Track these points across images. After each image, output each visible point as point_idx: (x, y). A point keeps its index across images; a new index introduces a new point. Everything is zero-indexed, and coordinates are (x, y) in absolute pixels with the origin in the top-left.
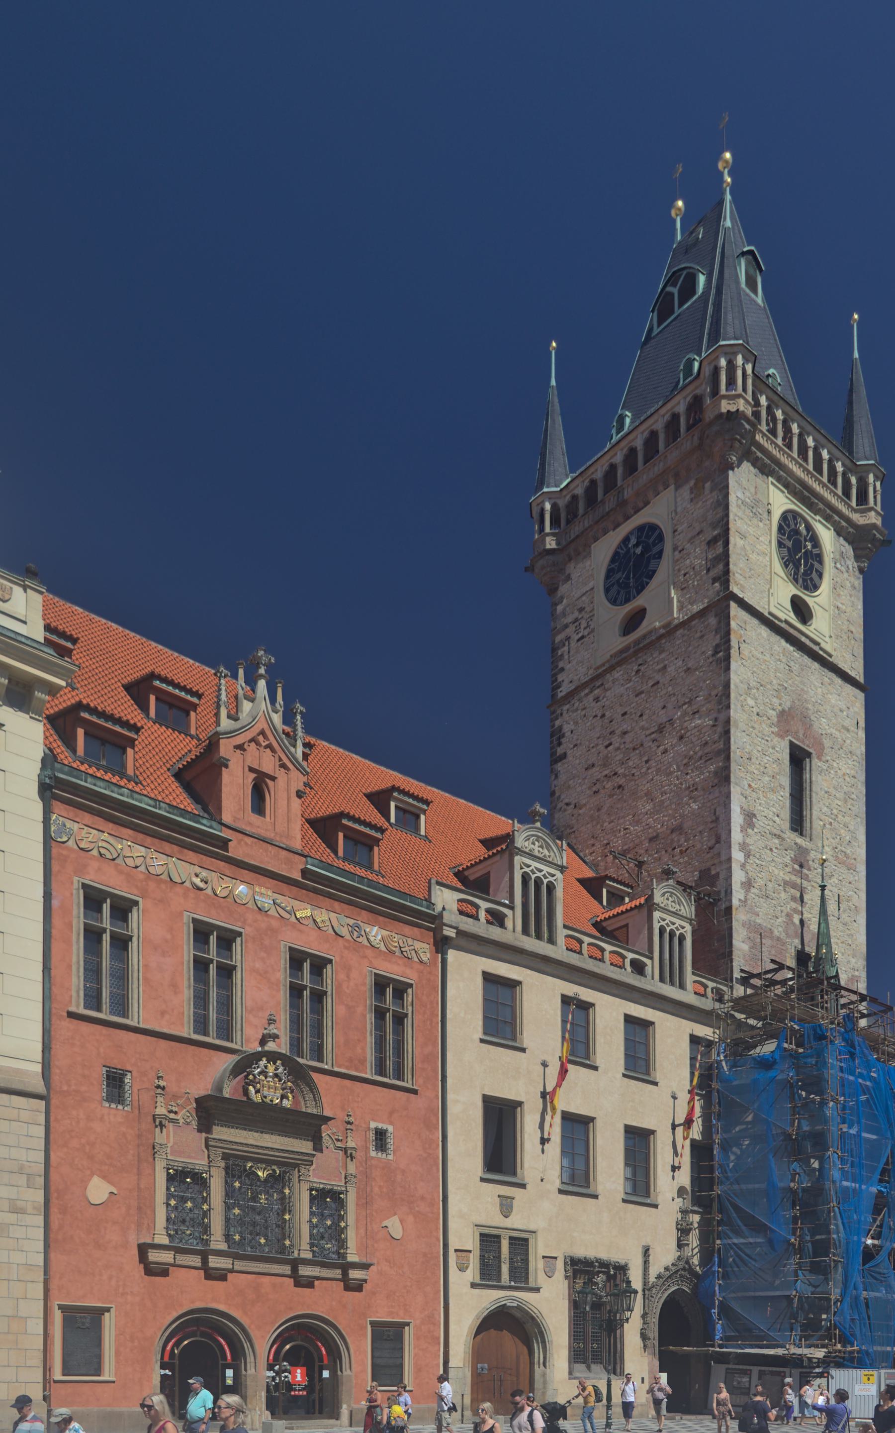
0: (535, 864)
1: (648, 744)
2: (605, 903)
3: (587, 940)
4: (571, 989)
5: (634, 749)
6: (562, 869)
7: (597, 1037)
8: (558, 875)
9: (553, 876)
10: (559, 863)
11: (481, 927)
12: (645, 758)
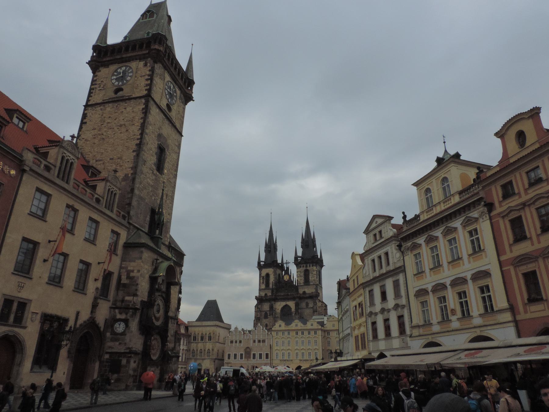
0: (68, 154)
1: (116, 129)
2: (90, 175)
3: (81, 186)
4: (71, 203)
5: (111, 129)
6: (78, 158)
7: (77, 223)
8: (76, 160)
9: (74, 160)
10: (77, 156)
11: (41, 170)
12: (114, 133)
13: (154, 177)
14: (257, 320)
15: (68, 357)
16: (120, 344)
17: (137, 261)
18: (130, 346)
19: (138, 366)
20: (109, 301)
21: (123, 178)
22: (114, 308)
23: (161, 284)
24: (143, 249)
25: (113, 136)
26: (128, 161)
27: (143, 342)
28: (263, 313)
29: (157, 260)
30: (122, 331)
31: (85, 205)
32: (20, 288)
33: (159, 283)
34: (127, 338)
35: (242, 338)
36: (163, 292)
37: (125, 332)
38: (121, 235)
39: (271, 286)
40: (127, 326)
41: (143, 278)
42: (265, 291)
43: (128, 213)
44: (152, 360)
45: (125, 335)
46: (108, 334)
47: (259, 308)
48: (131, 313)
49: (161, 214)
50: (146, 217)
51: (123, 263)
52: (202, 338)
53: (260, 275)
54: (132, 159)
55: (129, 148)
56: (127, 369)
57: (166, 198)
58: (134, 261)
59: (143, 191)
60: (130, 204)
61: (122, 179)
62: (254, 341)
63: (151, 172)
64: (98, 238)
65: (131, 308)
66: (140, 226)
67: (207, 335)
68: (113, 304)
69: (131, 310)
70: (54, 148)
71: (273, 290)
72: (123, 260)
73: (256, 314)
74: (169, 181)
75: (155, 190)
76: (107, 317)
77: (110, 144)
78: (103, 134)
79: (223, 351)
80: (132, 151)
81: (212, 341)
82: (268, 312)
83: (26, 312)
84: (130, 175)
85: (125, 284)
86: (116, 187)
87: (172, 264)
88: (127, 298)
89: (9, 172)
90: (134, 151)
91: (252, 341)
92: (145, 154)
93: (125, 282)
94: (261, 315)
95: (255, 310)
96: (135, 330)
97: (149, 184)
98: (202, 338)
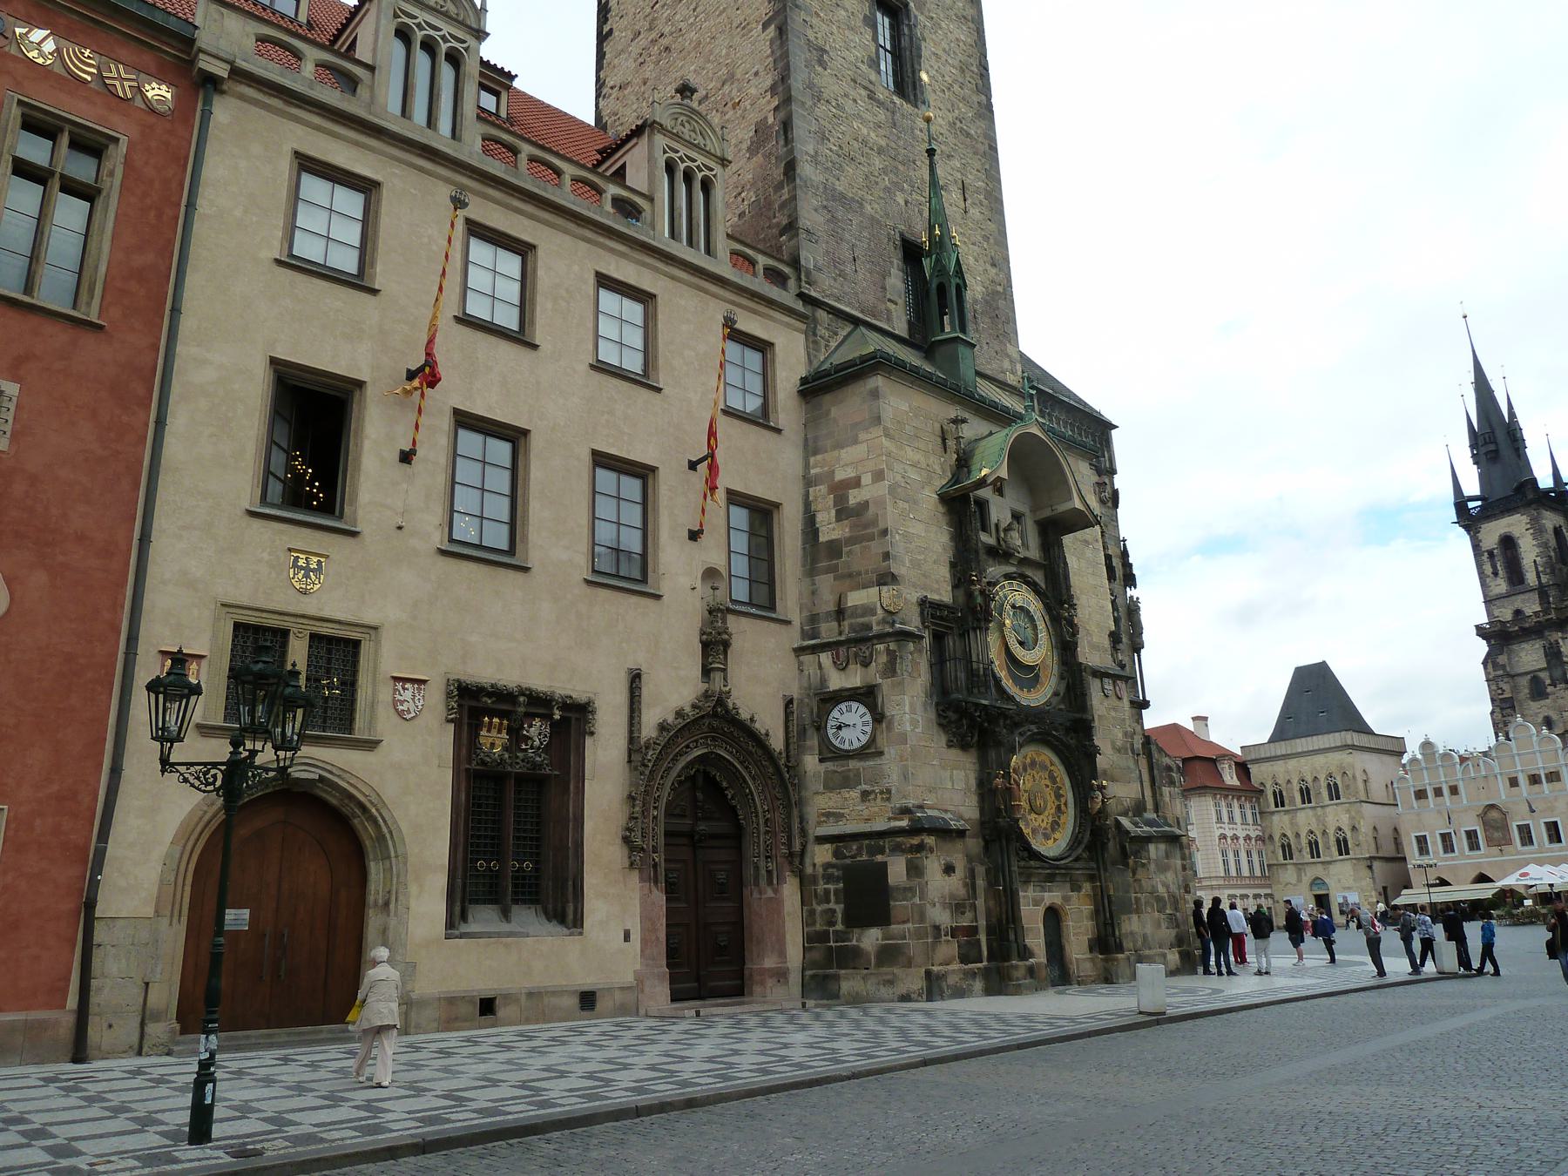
7: (539, 299)
10: (474, 26)
13: (882, 116)
14: (1502, 709)
15: (632, 864)
16: (865, 795)
17: (862, 436)
18: (911, 802)
19: (971, 886)
20: (788, 623)
21: (752, 143)
22: (814, 649)
23: (1008, 529)
24: (878, 381)
25: (692, 20)
26: (756, 74)
27: (973, 782)
28: (1524, 682)
29: (957, 421)
30: (864, 739)
31: (560, 221)
32: (307, 576)
33: (997, 526)
34: (890, 766)
35: (1459, 776)
36: (1025, 562)
37: (879, 740)
38: (777, 348)
39: (1531, 578)
40: (878, 717)
41: (906, 506)
42: (1513, 598)
43: (795, 263)
44: (1036, 856)
45: (881, 753)
46: (811, 762)
47: (1503, 667)
48: (883, 659)
49: (940, 244)
50: (884, 275)
51: (812, 460)
52: (1306, 795)
53: (1476, 547)
54: (768, 57)
55: (748, 24)
56: (917, 900)
57: (965, 200)
58: (855, 442)
59: (841, 169)
60: (791, 227)
61: (749, 148)
62: (1514, 782)
63: (864, 93)
64: (661, 362)
65: (881, 637)
66: (862, 312)
67: (1323, 784)
68: (805, 635)
69: (881, 647)
70: (368, 10)
71: (1542, 591)
72: (810, 448)
73: (1494, 687)
74: (961, 130)
75: (901, 168)
76: (795, 692)
77: (689, 53)
78: (662, 35)
79: (1395, 829)
80: (760, 27)
81: (1342, 800)
82: (1544, 676)
83: (363, 680)
84: (771, 120)
85: (831, 542)
86: (708, 154)
87: (1035, 430)
88: (855, 599)
89: (139, 90)
90: (765, 26)
91: (1502, 785)
92: (815, 21)
93: (835, 535)
94: (1515, 688)
95: (1487, 674)
96: (919, 730)
97: (865, 142)
98: (1306, 795)
